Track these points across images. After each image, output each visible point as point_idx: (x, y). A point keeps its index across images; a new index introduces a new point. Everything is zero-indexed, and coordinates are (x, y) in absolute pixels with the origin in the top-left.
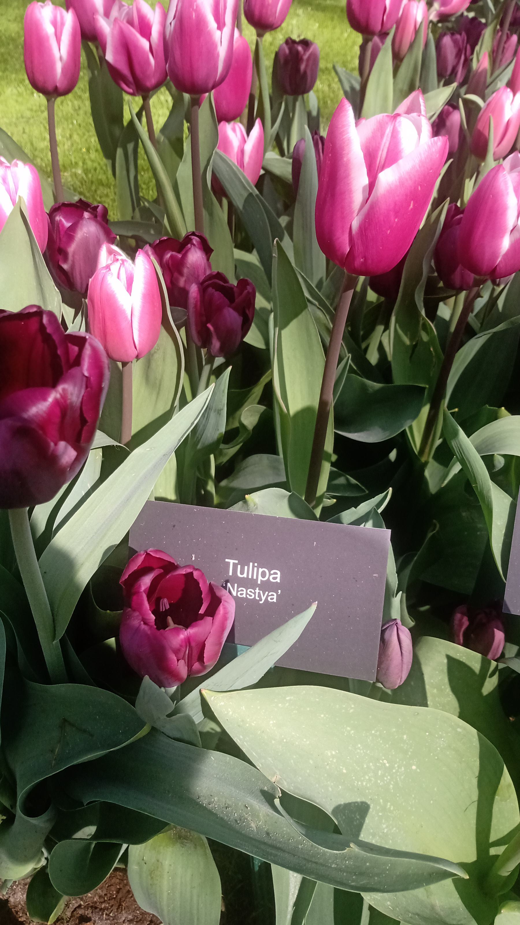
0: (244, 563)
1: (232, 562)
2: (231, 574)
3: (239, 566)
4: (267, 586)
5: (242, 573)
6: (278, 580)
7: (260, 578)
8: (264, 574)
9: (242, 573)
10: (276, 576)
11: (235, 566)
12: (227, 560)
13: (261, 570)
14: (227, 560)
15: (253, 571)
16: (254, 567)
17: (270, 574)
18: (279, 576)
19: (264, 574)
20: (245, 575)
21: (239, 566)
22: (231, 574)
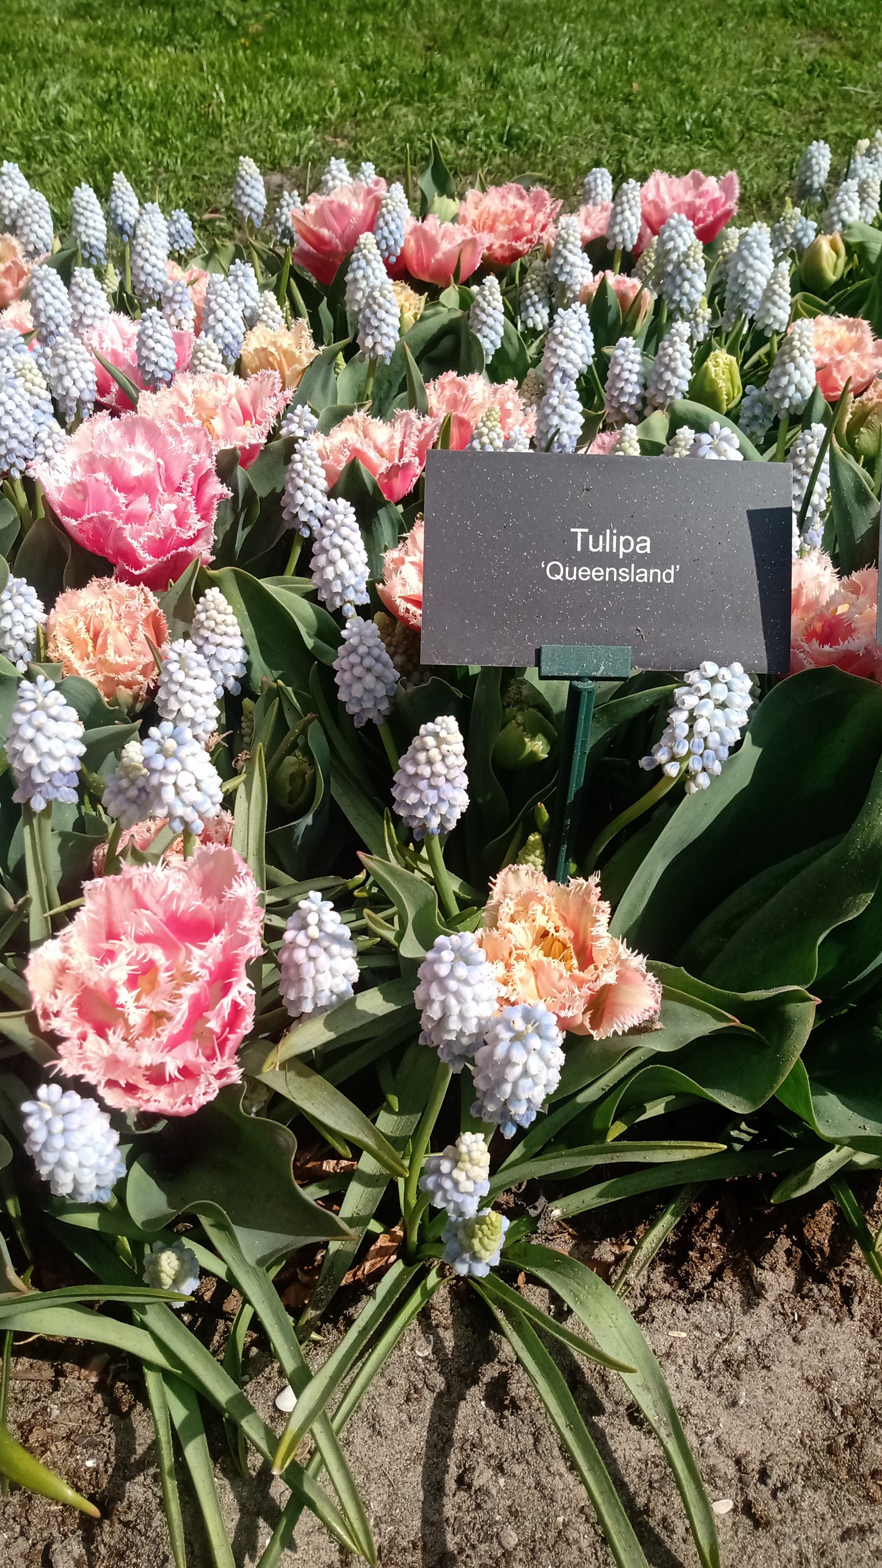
1: (579, 531)
4: (633, 559)
5: (596, 546)
6: (648, 550)
7: (622, 550)
8: (627, 544)
9: (596, 546)
10: (645, 545)
11: (585, 537)
13: (622, 539)
15: (610, 542)
16: (612, 534)
17: (636, 544)
18: (648, 544)
19: (627, 544)
20: (600, 549)
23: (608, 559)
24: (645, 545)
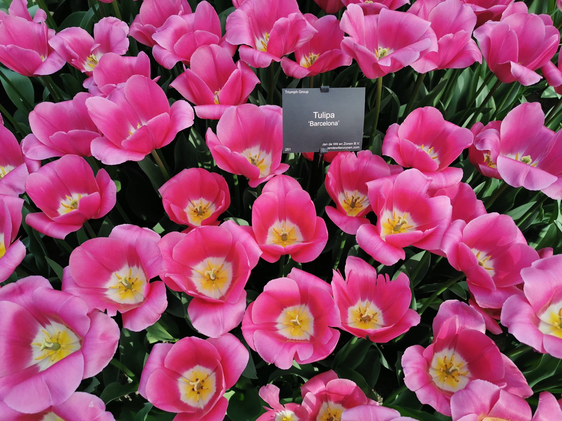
0: (320, 113)
1: (316, 113)
4: (330, 120)
8: (328, 116)
10: (333, 116)
11: (317, 114)
19: (328, 116)
23: (323, 120)
24: (333, 116)
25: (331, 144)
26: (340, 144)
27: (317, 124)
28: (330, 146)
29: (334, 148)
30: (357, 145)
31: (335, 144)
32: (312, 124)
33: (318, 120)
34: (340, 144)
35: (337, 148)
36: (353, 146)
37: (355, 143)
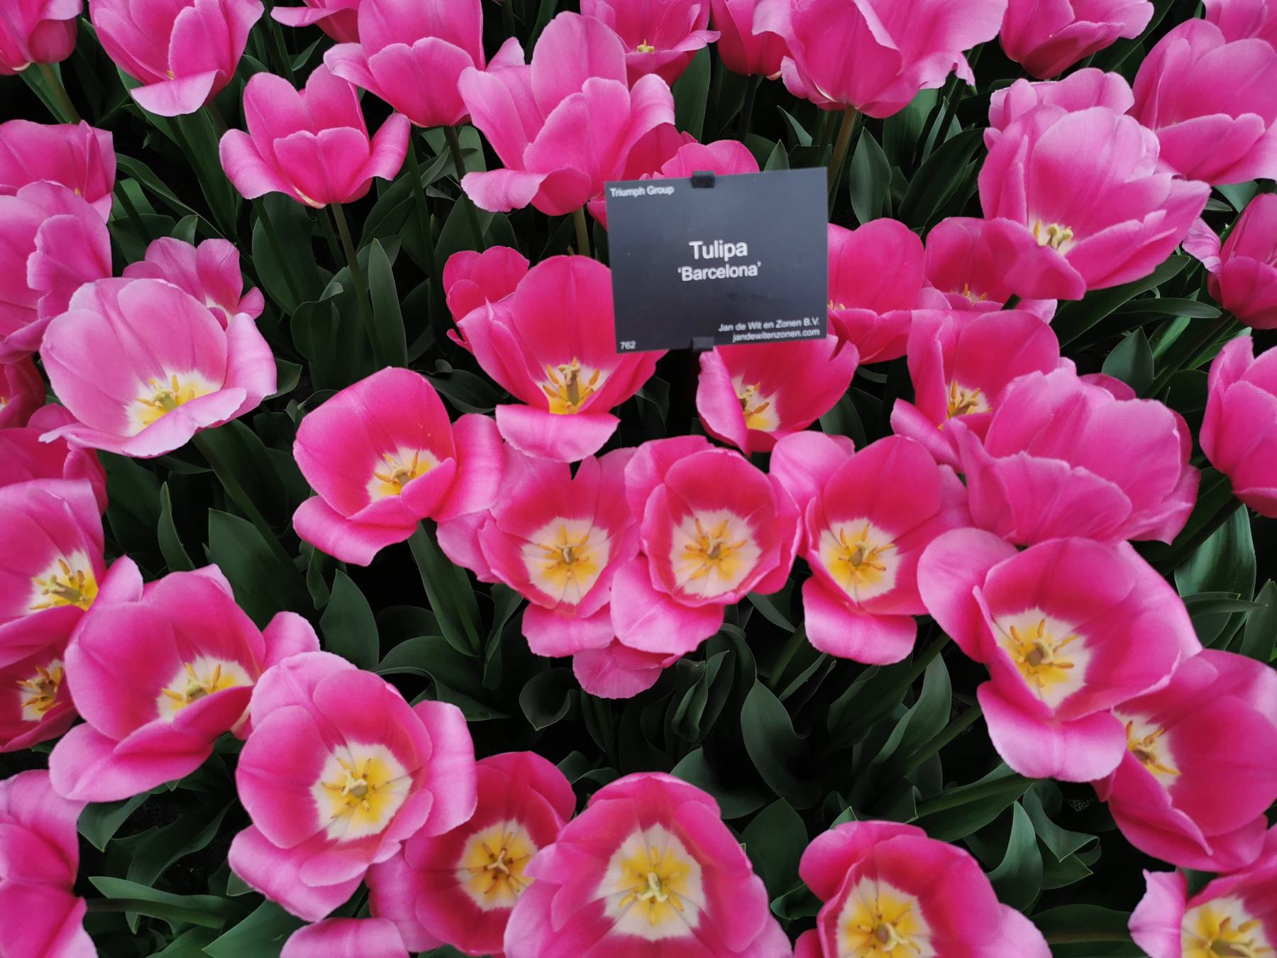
0: (708, 243)
1: (696, 244)
2: (697, 256)
3: (704, 248)
4: (735, 261)
6: (745, 253)
8: (730, 250)
10: (742, 249)
11: (700, 247)
12: (691, 244)
13: (727, 246)
14: (691, 244)
15: (719, 249)
19: (730, 250)
20: (711, 256)
21: (704, 248)
22: (697, 256)
23: (718, 262)
24: (742, 249)
25: (741, 327)
26: (767, 326)
27: (700, 275)
28: (741, 332)
29: (751, 337)
30: (812, 327)
31: (752, 325)
32: (687, 274)
33: (702, 264)
34: (767, 326)
35: (758, 337)
36: (802, 328)
37: (807, 322)
